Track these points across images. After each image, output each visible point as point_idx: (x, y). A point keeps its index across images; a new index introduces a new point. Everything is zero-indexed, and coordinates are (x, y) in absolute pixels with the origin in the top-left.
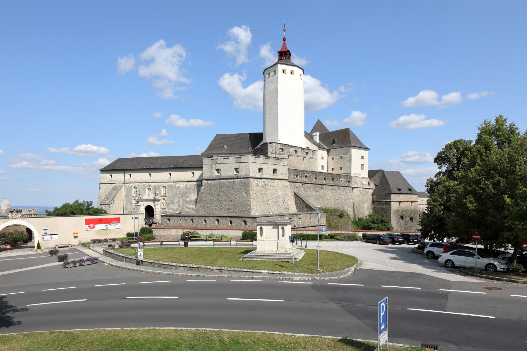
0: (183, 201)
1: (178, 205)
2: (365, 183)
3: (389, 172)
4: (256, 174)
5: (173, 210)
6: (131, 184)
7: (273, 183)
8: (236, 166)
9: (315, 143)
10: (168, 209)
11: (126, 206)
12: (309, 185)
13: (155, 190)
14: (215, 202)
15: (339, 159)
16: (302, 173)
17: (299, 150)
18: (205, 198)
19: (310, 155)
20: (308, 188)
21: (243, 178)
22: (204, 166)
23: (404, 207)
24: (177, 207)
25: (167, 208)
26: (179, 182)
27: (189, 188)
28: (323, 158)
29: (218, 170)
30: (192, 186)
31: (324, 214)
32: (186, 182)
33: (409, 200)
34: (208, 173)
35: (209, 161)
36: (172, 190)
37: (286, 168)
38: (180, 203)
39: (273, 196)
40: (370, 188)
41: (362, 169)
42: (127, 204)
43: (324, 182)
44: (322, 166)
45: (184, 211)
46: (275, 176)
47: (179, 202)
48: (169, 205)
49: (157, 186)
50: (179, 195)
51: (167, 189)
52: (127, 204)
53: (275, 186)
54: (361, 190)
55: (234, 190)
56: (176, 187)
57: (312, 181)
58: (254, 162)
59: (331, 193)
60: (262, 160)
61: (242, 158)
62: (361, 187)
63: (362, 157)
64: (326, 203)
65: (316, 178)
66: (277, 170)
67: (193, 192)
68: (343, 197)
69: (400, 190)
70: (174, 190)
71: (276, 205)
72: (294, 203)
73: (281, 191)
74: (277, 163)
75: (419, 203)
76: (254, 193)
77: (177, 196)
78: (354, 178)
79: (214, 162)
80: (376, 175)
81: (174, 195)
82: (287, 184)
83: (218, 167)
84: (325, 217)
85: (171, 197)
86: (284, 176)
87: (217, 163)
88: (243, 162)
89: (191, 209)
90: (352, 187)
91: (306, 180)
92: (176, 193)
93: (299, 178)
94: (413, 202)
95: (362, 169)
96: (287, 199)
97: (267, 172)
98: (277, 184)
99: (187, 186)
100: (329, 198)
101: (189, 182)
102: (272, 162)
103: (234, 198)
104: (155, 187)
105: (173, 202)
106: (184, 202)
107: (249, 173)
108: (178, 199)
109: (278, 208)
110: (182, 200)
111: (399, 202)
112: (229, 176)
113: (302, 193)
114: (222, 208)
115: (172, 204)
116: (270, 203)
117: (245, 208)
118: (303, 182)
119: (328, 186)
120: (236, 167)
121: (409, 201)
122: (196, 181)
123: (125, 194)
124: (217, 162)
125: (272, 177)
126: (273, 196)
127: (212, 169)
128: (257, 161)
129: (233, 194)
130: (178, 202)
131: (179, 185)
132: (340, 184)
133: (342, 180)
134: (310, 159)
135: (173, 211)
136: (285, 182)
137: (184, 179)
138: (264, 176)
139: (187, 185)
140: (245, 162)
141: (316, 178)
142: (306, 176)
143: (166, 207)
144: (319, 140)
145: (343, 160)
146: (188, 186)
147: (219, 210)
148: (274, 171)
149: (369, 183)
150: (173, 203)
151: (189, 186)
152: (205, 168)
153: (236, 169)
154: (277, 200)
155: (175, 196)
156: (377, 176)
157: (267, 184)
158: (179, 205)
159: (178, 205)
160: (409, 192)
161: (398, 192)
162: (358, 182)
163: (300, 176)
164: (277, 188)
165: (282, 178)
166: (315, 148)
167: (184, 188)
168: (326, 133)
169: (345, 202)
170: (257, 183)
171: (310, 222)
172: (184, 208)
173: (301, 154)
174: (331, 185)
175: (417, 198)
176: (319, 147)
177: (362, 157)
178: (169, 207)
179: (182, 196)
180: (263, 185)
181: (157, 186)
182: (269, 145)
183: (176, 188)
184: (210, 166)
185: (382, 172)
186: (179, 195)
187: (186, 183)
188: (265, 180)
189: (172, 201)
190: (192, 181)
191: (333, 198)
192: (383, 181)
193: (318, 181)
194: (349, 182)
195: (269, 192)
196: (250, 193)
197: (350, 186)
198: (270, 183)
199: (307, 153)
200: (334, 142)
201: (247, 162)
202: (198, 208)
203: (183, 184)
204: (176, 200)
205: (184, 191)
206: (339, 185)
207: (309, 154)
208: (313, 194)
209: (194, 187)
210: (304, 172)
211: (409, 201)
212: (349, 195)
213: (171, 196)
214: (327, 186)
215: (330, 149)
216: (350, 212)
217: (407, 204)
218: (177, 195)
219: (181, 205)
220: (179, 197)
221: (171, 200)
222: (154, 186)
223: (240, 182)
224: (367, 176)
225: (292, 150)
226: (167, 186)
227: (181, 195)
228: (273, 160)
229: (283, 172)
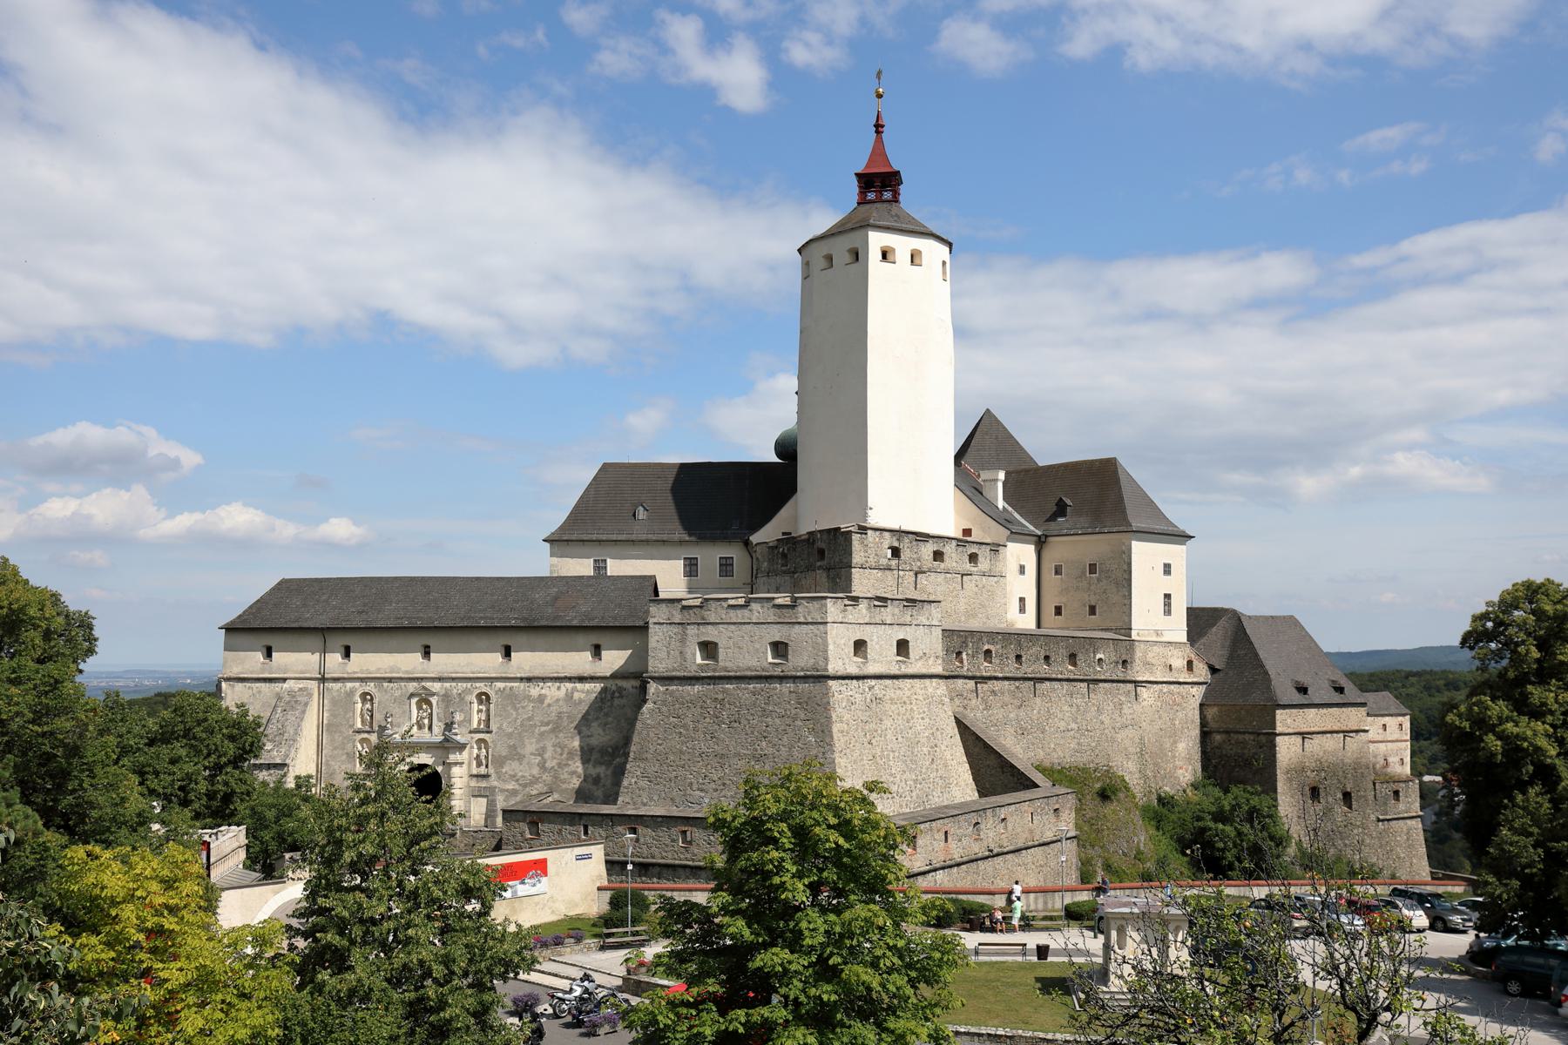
0: (559, 750)
1: (538, 765)
2: (1179, 662)
3: (1257, 618)
4: (847, 661)
5: (517, 780)
6: (349, 685)
7: (898, 692)
8: (777, 634)
9: (986, 507)
10: (499, 778)
11: (327, 764)
12: (997, 685)
13: (447, 707)
14: (699, 759)
15: (1084, 573)
16: (973, 643)
17: (949, 549)
18: (660, 745)
19: (984, 564)
20: (996, 695)
21: (805, 678)
22: (653, 629)
23: (1321, 754)
24: (536, 771)
25: (493, 776)
28: (1022, 570)
29: (709, 649)
31: (1069, 796)
33: (1336, 728)
34: (668, 653)
35: (674, 612)
36: (516, 709)
37: (938, 632)
38: (547, 756)
39: (900, 739)
40: (1195, 680)
41: (1168, 610)
42: (333, 757)
43: (1043, 669)
44: (1022, 600)
45: (564, 786)
46: (903, 666)
47: (541, 752)
48: (504, 763)
49: (455, 691)
50: (543, 729)
51: (497, 705)
52: (333, 757)
53: (905, 703)
54: (1165, 690)
55: (769, 719)
56: (529, 698)
57: (1006, 669)
58: (840, 620)
59: (1066, 708)
60: (864, 611)
61: (800, 609)
62: (1165, 680)
63: (1167, 569)
64: (1052, 746)
65: (1018, 657)
66: (910, 644)
67: (597, 719)
68: (1107, 721)
69: (1303, 690)
70: (523, 708)
71: (911, 770)
72: (965, 759)
73: (923, 719)
74: (908, 619)
75: (1371, 735)
76: (842, 732)
77: (533, 732)
78: (1142, 646)
79: (693, 615)
80: (1214, 629)
81: (522, 725)
82: (938, 692)
83: (710, 634)
84: (1071, 809)
85: (510, 736)
86: (931, 662)
87: (703, 619)
88: (802, 620)
90: (1135, 682)
91: (986, 668)
92: (529, 719)
93: (965, 662)
94: (1351, 735)
95: (1168, 610)
96: (943, 748)
97: (882, 658)
98: (908, 693)
100: (1062, 725)
101: (581, 679)
102: (893, 615)
104: (446, 698)
105: (518, 754)
106: (561, 754)
107: (826, 659)
108: (537, 742)
109: (915, 781)
110: (554, 746)
111: (1304, 735)
112: (749, 669)
113: (977, 719)
114: (728, 782)
115: (514, 760)
116: (891, 763)
118: (978, 674)
119: (1056, 685)
120: (777, 639)
121: (1337, 732)
122: (608, 674)
123: (325, 722)
125: (894, 671)
126: (900, 739)
127: (683, 641)
128: (850, 618)
129: (765, 734)
130: (539, 755)
131: (543, 691)
132: (1096, 672)
133: (1101, 656)
134: (984, 578)
135: (517, 787)
136: (934, 684)
137: (563, 667)
138: (872, 669)
139: (574, 689)
140: (810, 620)
141: (1018, 657)
142: (988, 652)
143: (491, 770)
144: (1005, 499)
145: (1099, 580)
146: (576, 696)
147: (716, 790)
148: (903, 647)
149: (1190, 663)
150: (520, 758)
151: (583, 696)
152: (657, 638)
153: (780, 648)
154: (913, 753)
156: (1217, 634)
157: (881, 696)
158: (542, 766)
159: (538, 765)
160: (1337, 698)
161: (1298, 698)
162: (1154, 661)
163: (970, 652)
164: (912, 709)
165: (924, 671)
166: (996, 533)
167: (561, 702)
168: (1027, 471)
169: (1113, 740)
170: (851, 693)
171: (1031, 831)
172: (562, 777)
173: (954, 564)
174: (1068, 680)
175: (1364, 718)
176: (1012, 532)
177: (1167, 569)
178: (504, 770)
179: (553, 731)
180: (868, 700)
181: (455, 691)
182: (855, 537)
183: (533, 701)
185: (1236, 617)
186: (543, 729)
187: (569, 685)
188: (873, 682)
189: (514, 747)
191: (1074, 726)
192: (1238, 656)
193: (1027, 669)
194: (1125, 662)
195: (887, 723)
196: (830, 732)
197: (1128, 678)
198: (890, 693)
199: (973, 558)
200: (1061, 510)
202: (633, 781)
203: (559, 688)
204: (530, 747)
206: (1092, 677)
207: (981, 559)
208: (1012, 715)
210: (981, 639)
211: (1337, 732)
212: (1126, 710)
213: (510, 730)
214: (1054, 683)
215: (1046, 536)
216: (1129, 770)
217: (1331, 743)
218: (535, 726)
219: (548, 765)
220: (542, 734)
221: (510, 747)
222: (443, 692)
224: (1183, 637)
225: (928, 549)
226: (496, 694)
228: (896, 611)
229: (928, 651)
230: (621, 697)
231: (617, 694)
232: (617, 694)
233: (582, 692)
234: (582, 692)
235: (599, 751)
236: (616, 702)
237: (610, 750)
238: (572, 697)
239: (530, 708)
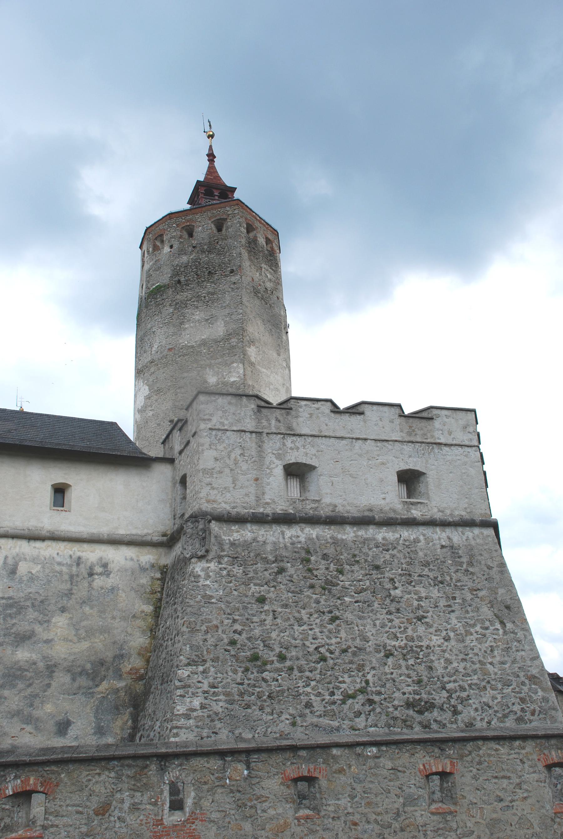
27: (32, 578)
32: (14, 537)
61: (437, 424)
67: (63, 610)
79: (273, 422)
87: (290, 428)
89: (51, 726)
103: (434, 638)
114: (376, 698)
117: (523, 700)
124: (294, 425)
146: (23, 568)
151: (36, 568)
152: (214, 453)
184: (250, 442)
190: (54, 538)
201: (467, 443)
202: (196, 703)
209: (72, 577)
223: (443, 547)
233: (35, 560)
235: (68, 670)
237: (88, 666)
238: (13, 571)
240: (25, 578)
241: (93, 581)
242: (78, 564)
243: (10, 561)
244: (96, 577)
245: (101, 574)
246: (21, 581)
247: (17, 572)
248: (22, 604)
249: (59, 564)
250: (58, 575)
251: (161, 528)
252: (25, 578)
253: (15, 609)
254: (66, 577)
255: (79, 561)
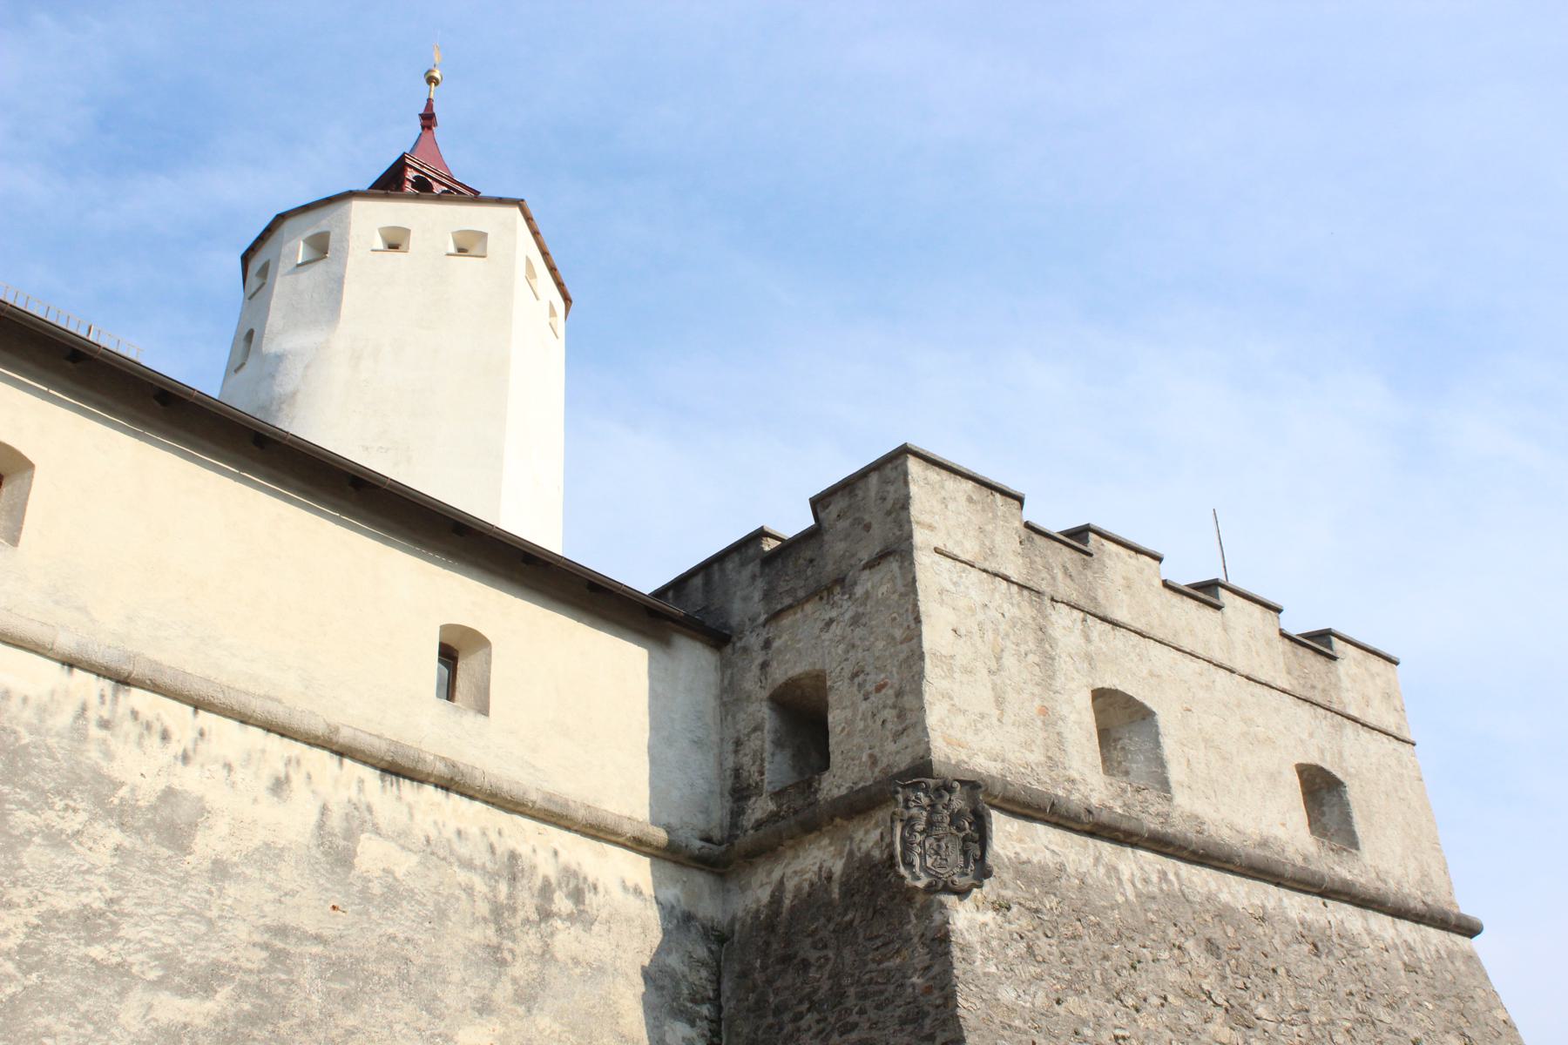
26: (198, 704)
27: (394, 895)
30: (463, 876)
70: (56, 840)
92: (89, 923)
99: (350, 835)
131: (190, 780)
139: (360, 820)
146: (371, 854)
151: (405, 864)
155: (60, 1004)
167: (288, 874)
183: (122, 816)
203: (279, 786)
205: (282, 931)
209: (499, 914)
227: (224, 992)
230: (580, 917)
231: (562, 903)
232: (562, 903)
233: (401, 838)
234: (401, 838)
236: (566, 939)
238: (343, 859)
239: (103, 857)
240: (376, 888)
241: (552, 934)
242: (513, 879)
243: (336, 822)
244: (558, 923)
245: (571, 918)
246: (365, 896)
247: (356, 861)
248: (372, 967)
249: (468, 865)
250: (463, 896)
251: (699, 821)
252: (376, 888)
253: (353, 983)
254: (483, 909)
255: (513, 867)
